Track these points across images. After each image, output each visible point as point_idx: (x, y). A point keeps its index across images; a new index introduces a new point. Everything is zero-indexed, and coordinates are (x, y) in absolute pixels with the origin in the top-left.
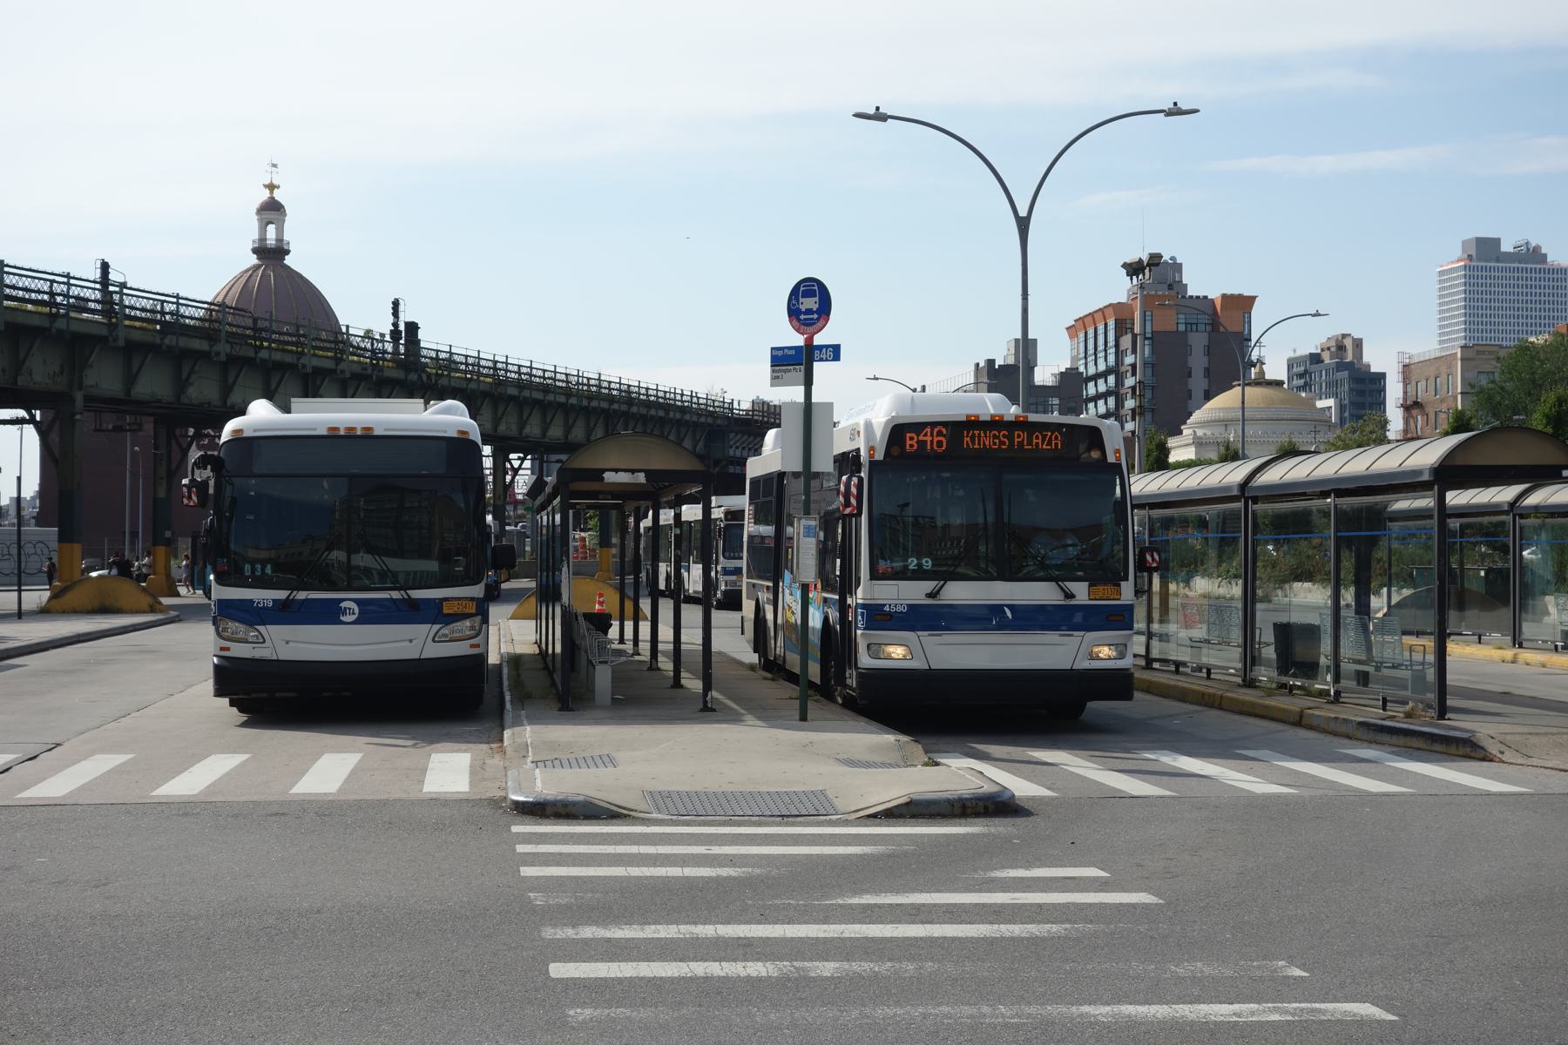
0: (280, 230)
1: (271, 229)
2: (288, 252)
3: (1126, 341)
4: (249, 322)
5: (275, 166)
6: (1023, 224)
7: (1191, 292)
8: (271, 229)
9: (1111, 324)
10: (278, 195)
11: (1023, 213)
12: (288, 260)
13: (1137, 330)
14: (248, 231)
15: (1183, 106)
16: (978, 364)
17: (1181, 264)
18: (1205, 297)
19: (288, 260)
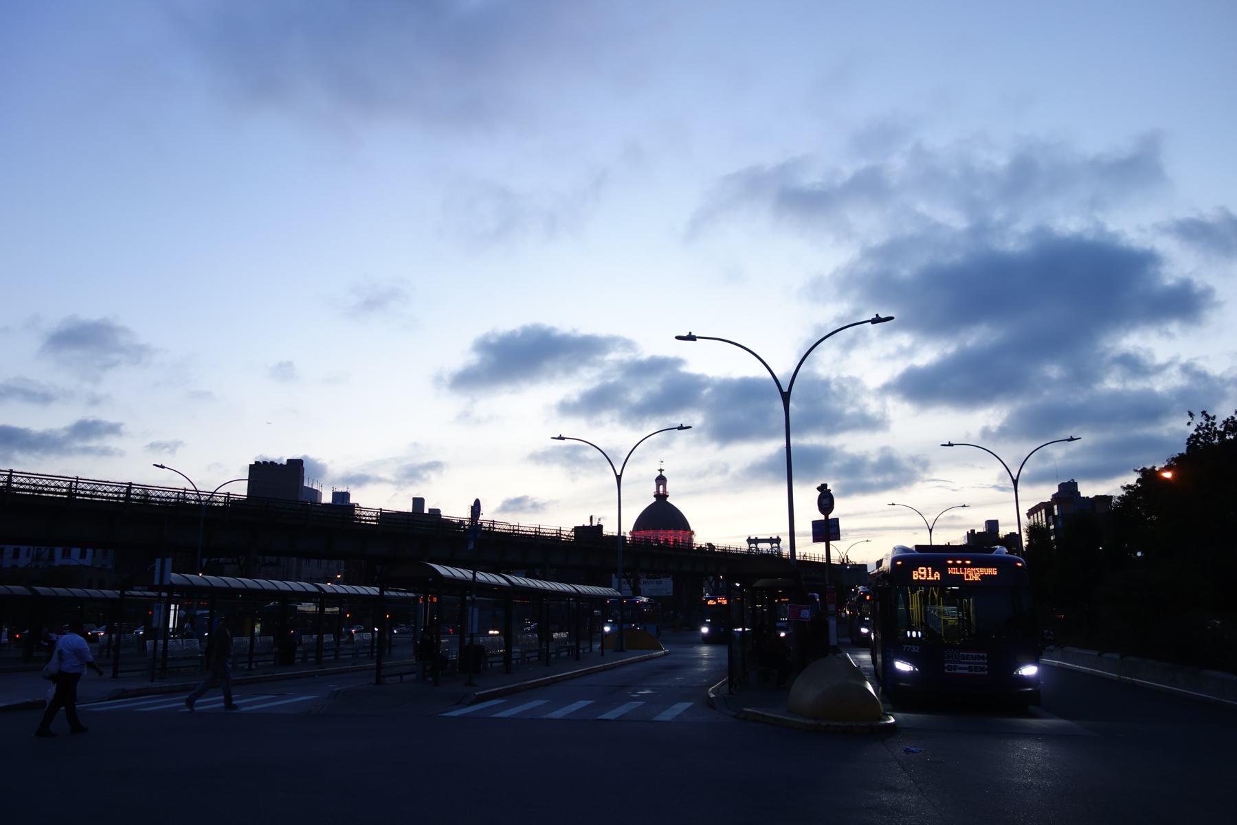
0: (665, 488)
1: (661, 487)
2: (668, 496)
3: (1051, 518)
4: (508, 527)
5: (662, 462)
6: (619, 478)
7: (1082, 495)
8: (661, 487)
9: (1043, 511)
10: (663, 473)
11: (619, 473)
12: (668, 500)
13: (1056, 513)
14: (652, 488)
15: (684, 426)
16: (968, 532)
17: (1076, 483)
18: (1088, 497)
19: (668, 500)
